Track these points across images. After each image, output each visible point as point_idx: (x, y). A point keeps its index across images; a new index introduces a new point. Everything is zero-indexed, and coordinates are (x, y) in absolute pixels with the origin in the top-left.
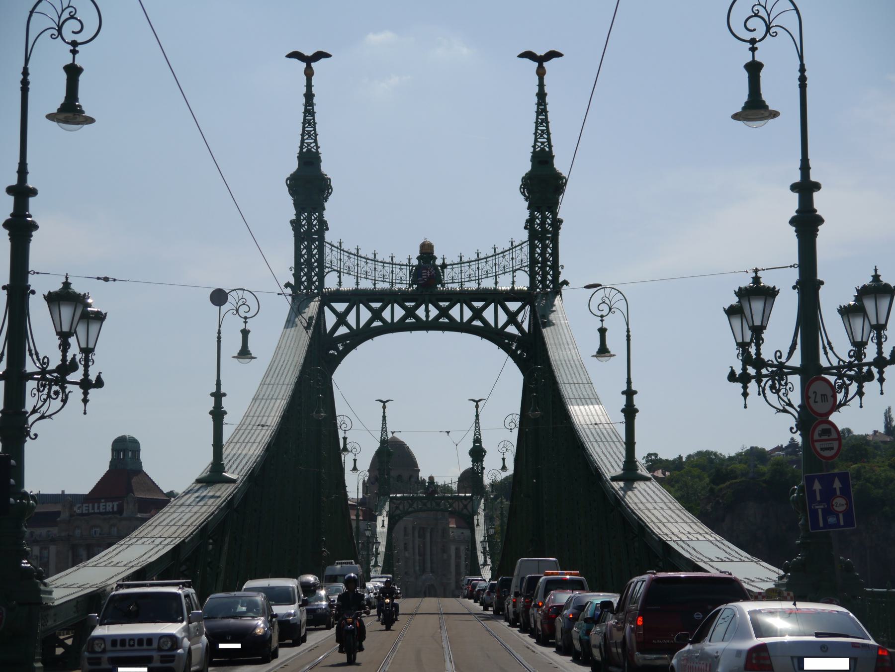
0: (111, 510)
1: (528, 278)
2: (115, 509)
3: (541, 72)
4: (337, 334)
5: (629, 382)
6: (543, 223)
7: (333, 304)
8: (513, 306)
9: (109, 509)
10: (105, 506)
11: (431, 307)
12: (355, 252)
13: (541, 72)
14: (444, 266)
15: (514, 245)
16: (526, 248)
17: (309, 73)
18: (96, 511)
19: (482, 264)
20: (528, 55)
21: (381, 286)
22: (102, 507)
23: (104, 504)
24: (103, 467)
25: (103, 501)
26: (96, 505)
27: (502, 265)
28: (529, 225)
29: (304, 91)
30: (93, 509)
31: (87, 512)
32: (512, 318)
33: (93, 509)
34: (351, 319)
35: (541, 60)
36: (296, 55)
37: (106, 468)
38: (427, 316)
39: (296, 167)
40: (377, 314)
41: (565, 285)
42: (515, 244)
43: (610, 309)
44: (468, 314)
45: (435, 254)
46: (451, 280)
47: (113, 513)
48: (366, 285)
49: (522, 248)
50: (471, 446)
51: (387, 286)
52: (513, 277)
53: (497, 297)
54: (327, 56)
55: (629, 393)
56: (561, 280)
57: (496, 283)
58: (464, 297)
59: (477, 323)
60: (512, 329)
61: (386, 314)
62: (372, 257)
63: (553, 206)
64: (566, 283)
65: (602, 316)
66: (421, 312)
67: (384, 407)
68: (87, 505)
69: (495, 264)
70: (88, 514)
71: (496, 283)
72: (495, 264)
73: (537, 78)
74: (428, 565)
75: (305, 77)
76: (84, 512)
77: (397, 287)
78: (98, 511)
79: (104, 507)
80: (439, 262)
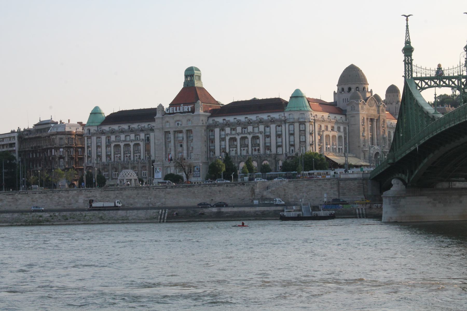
0: (187, 111)
2: (190, 110)
9: (186, 110)
10: (184, 108)
18: (178, 111)
22: (181, 109)
23: (183, 107)
24: (180, 86)
25: (182, 105)
26: (178, 108)
30: (176, 110)
31: (172, 112)
33: (176, 110)
37: (182, 86)
47: (188, 112)
67: (407, 20)
68: (172, 108)
70: (173, 113)
76: (171, 112)
78: (179, 111)
79: (183, 109)
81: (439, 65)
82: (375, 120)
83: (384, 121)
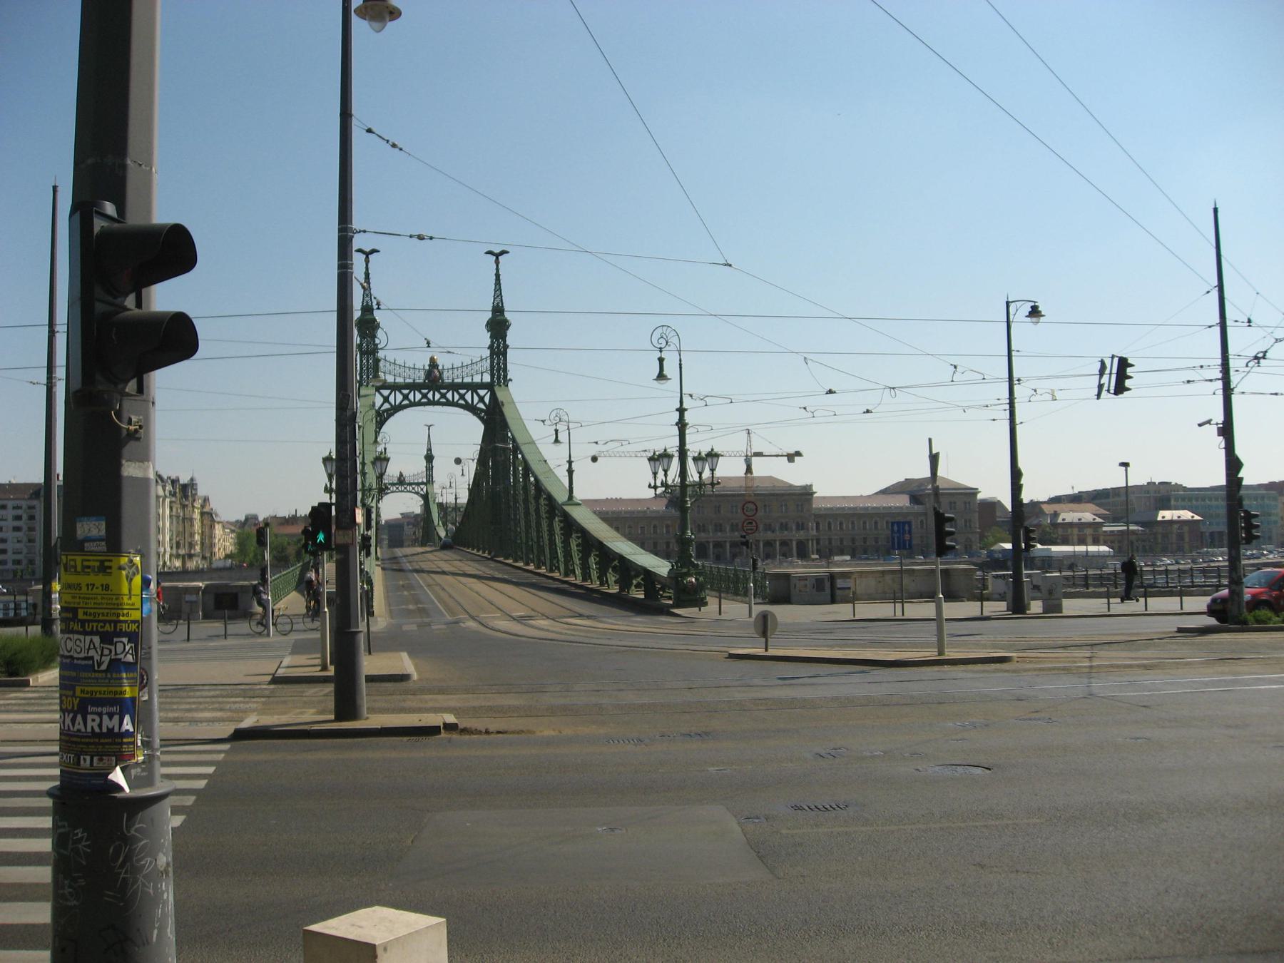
1: (489, 377)
3: (497, 262)
4: (382, 409)
6: (498, 346)
7: (381, 391)
8: (482, 392)
11: (436, 393)
13: (497, 262)
14: (443, 369)
16: (489, 361)
19: (465, 369)
21: (408, 381)
28: (491, 347)
32: (481, 399)
34: (391, 399)
35: (497, 255)
38: (434, 398)
40: (406, 397)
44: (456, 397)
46: (448, 378)
48: (399, 380)
51: (411, 381)
52: (482, 375)
53: (473, 387)
54: (378, 251)
56: (508, 378)
57: (472, 379)
58: (455, 387)
59: (462, 402)
60: (481, 406)
61: (411, 396)
63: (504, 337)
64: (511, 380)
65: (661, 348)
66: (430, 396)
71: (472, 379)
77: (417, 381)
80: (440, 368)
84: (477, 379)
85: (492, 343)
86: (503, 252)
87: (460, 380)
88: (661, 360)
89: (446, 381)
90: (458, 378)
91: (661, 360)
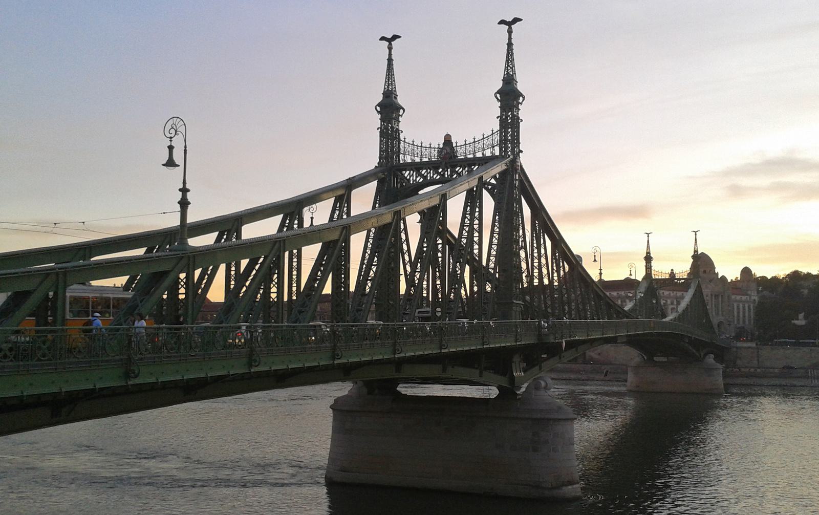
3: (510, 32)
5: (184, 183)
12: (412, 143)
13: (510, 32)
14: (456, 146)
15: (494, 132)
17: (390, 48)
19: (477, 144)
20: (502, 22)
27: (487, 144)
29: (387, 57)
35: (510, 24)
36: (383, 39)
39: (382, 99)
41: (521, 154)
42: (494, 132)
43: (176, 132)
45: (452, 141)
48: (417, 160)
49: (497, 134)
50: (692, 254)
51: (427, 160)
54: (399, 37)
55: (184, 191)
62: (420, 145)
65: (171, 138)
67: (648, 236)
69: (484, 144)
72: (484, 144)
73: (508, 34)
74: (720, 313)
75: (388, 50)
77: (433, 160)
81: (672, 270)
82: (721, 296)
83: (729, 297)
84: (488, 153)
85: (501, 117)
86: (516, 20)
87: (471, 156)
88: (171, 148)
89: (459, 158)
90: (470, 154)
91: (171, 148)
